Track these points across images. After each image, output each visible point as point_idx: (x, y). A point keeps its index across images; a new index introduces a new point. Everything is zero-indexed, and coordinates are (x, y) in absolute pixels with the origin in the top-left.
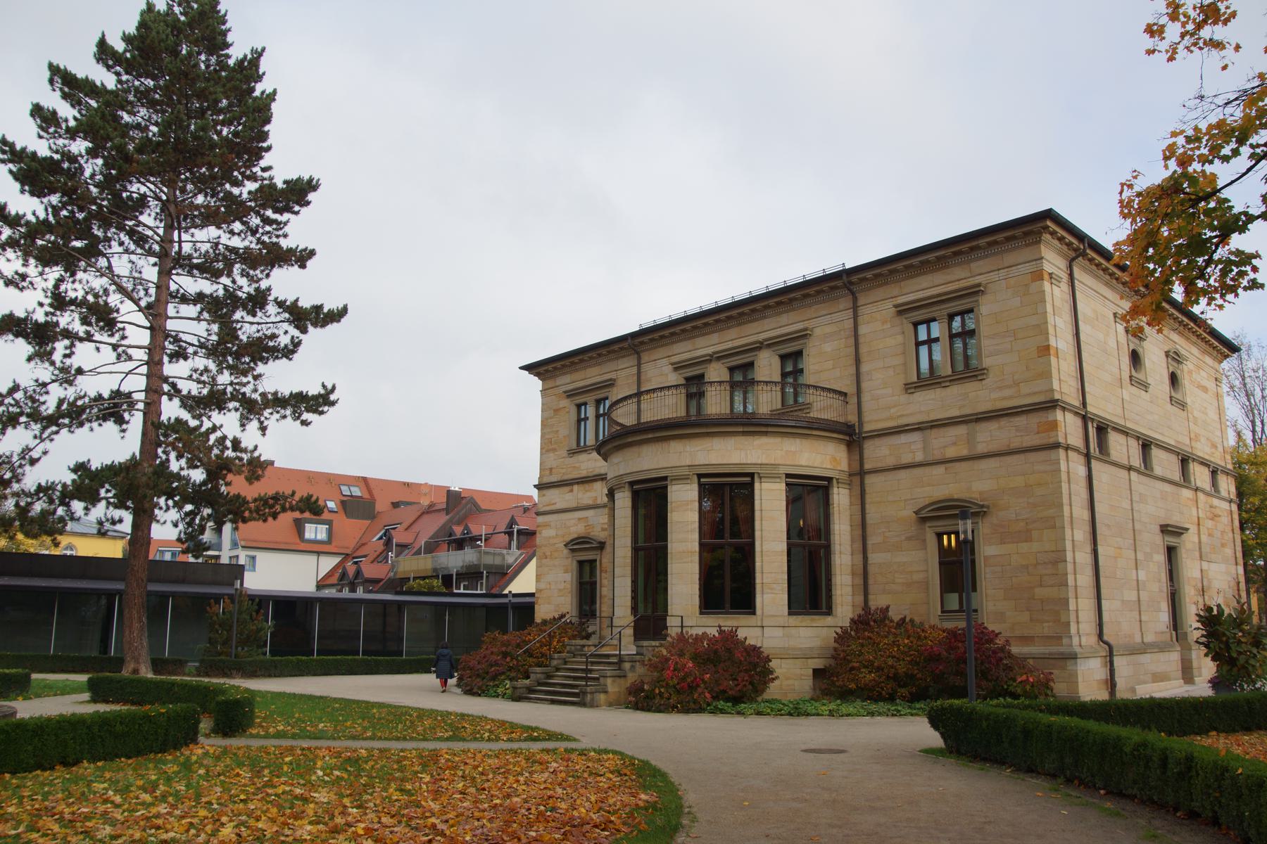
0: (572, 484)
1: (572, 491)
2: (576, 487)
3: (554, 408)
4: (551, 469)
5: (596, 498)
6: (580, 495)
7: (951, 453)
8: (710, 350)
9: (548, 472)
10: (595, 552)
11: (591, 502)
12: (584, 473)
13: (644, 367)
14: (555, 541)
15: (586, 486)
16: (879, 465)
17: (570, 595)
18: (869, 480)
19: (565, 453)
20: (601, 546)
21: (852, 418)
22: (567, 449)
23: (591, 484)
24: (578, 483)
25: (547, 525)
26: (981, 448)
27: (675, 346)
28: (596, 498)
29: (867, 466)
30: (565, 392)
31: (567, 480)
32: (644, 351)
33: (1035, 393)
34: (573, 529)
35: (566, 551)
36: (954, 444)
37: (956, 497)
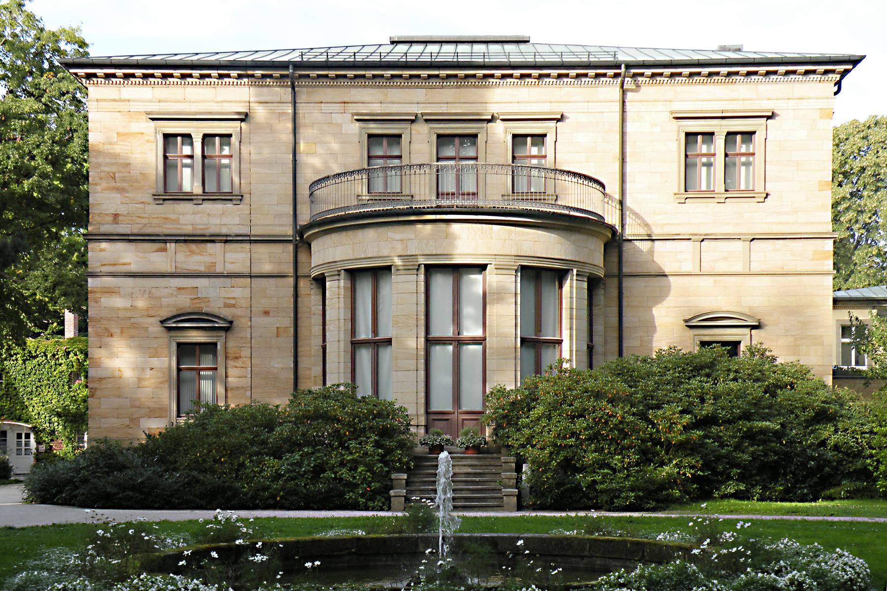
0: (165, 242)
1: (165, 250)
2: (171, 246)
3: (121, 130)
4: (116, 216)
5: (214, 264)
6: (181, 257)
7: (722, 268)
8: (419, 110)
9: (110, 219)
10: (214, 333)
11: (202, 269)
12: (188, 229)
13: (302, 109)
14: (129, 315)
15: (193, 246)
16: (639, 270)
17: (167, 386)
18: (627, 283)
19: (148, 198)
20: (228, 327)
21: (612, 218)
22: (154, 191)
23: (203, 245)
24: (177, 241)
25: (110, 291)
26: (755, 267)
27: (353, 91)
28: (214, 264)
29: (625, 270)
30: (148, 113)
31: (158, 235)
32: (300, 86)
33: (813, 223)
34: (171, 301)
35: (156, 329)
36: (725, 259)
37: (724, 309)
